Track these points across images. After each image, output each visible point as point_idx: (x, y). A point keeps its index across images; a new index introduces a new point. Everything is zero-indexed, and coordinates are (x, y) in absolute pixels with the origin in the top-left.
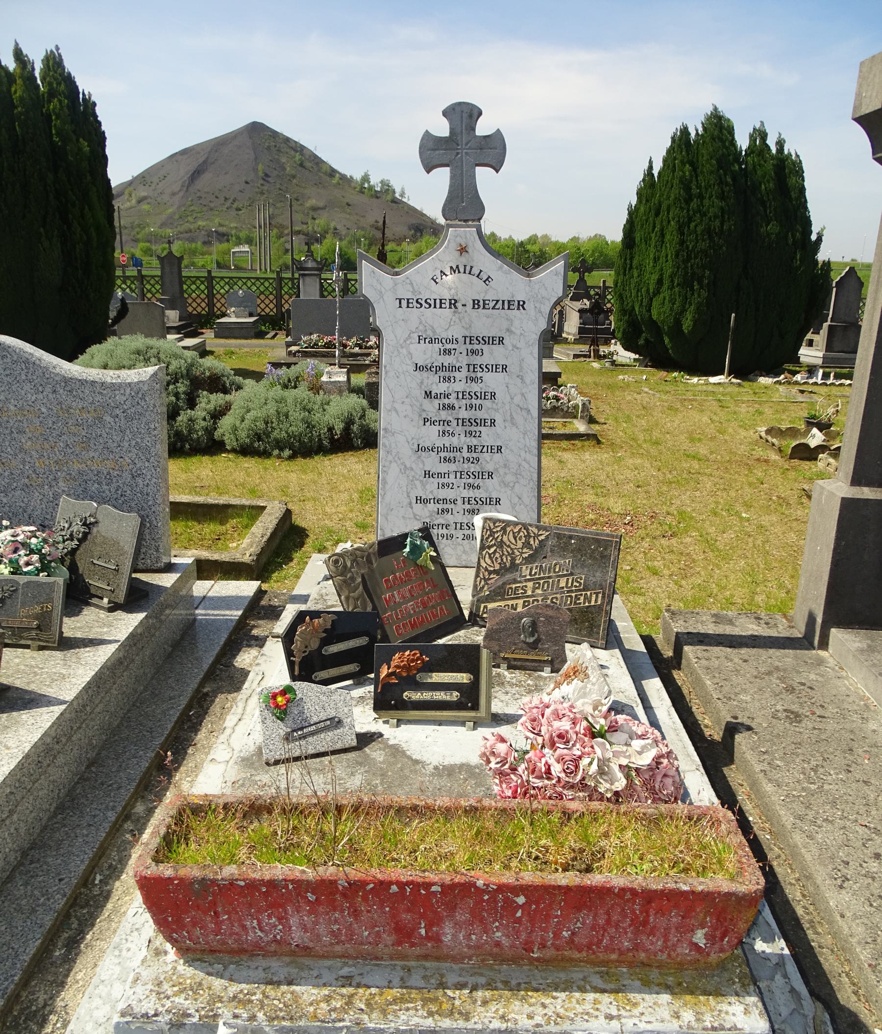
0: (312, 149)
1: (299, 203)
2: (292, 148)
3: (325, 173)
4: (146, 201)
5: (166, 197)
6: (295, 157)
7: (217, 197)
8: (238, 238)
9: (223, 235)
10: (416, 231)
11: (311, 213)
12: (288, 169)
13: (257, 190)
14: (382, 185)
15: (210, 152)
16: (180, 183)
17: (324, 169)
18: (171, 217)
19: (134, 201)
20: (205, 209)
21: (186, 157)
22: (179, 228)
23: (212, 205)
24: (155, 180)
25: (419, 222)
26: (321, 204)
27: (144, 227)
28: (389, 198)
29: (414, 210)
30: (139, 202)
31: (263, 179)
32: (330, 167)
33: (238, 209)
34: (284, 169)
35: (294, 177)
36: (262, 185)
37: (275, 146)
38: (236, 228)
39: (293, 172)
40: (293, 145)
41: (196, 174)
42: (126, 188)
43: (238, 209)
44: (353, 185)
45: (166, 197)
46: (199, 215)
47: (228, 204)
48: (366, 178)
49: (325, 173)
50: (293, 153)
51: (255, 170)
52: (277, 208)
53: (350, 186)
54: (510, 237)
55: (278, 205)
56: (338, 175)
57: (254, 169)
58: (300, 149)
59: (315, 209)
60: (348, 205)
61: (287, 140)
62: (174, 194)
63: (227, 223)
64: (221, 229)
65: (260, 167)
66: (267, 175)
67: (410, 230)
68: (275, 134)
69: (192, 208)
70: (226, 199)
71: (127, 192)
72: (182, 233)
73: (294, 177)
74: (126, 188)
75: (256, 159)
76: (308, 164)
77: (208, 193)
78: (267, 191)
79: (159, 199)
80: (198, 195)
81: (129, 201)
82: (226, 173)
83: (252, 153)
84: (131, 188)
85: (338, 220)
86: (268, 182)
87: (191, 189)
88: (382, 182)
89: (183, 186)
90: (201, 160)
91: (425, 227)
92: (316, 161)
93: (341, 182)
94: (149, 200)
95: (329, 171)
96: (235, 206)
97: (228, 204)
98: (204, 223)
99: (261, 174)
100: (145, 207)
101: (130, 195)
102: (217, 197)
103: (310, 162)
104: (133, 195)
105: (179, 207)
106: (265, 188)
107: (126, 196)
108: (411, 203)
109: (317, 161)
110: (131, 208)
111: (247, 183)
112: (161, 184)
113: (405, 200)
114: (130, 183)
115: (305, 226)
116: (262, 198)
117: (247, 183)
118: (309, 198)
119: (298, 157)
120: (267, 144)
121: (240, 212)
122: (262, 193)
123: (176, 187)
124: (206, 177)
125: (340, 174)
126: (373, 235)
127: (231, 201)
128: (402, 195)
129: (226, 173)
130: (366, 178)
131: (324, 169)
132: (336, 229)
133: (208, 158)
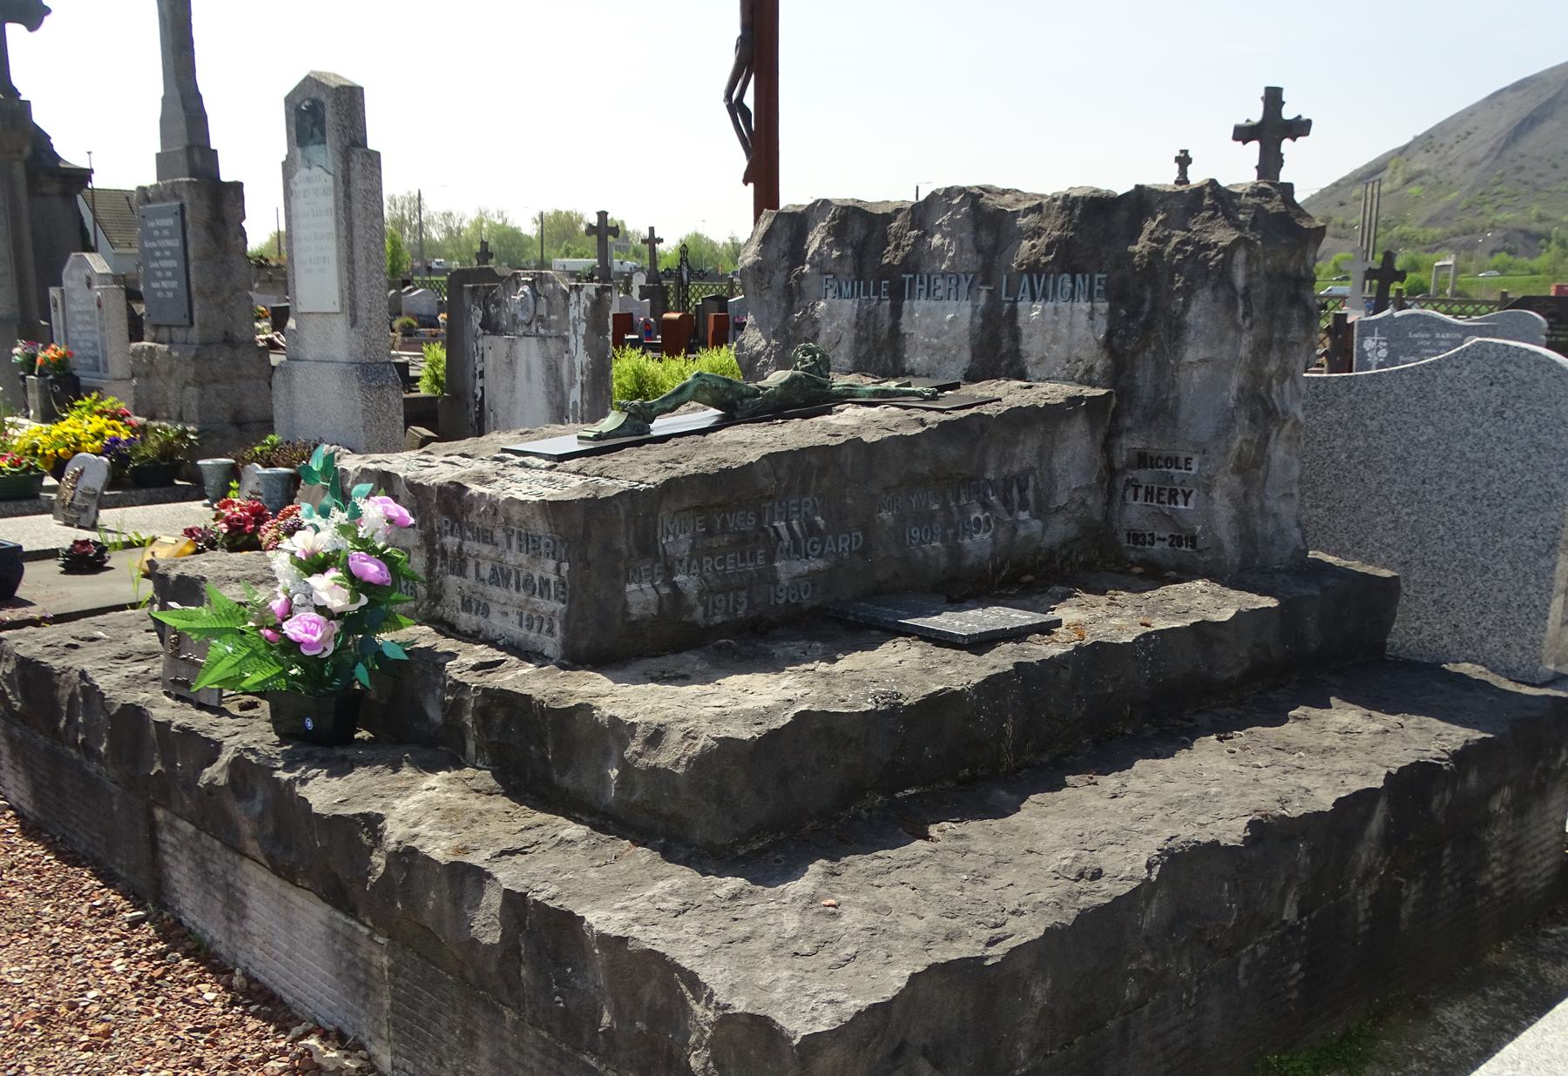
7: (1555, 166)
9: (1538, 237)
19: (1399, 180)
20: (1523, 190)
21: (1520, 93)
23: (1540, 181)
24: (1450, 140)
30: (1408, 181)
41: (1530, 123)
46: (1506, 201)
62: (1472, 165)
63: (1555, 214)
64: (1536, 227)
69: (1498, 188)
71: (1392, 164)
72: (1456, 235)
77: (1539, 159)
79: (1442, 176)
89: (1492, 149)
100: (1414, 190)
102: (1555, 166)
105: (1473, 189)
112: (1456, 148)
123: (1479, 153)
124: (1546, 129)
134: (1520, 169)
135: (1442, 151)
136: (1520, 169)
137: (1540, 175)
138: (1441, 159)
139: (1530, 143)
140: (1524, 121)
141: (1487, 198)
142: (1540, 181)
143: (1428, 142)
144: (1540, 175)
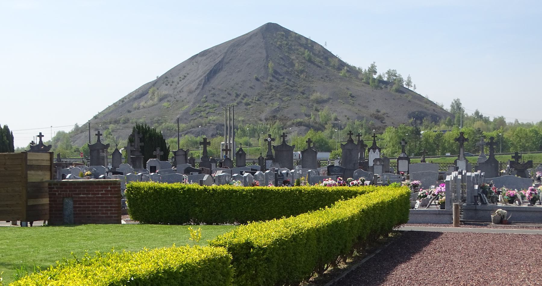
0: (323, 45)
1: (305, 96)
2: (301, 45)
3: (333, 67)
4: (166, 100)
5: (184, 95)
6: (304, 54)
7: (229, 94)
8: (243, 131)
10: (417, 119)
11: (315, 105)
12: (297, 65)
13: (266, 86)
14: (389, 75)
15: (226, 53)
16: (198, 81)
17: (332, 64)
18: (186, 113)
19: (156, 99)
20: (217, 105)
21: (205, 58)
22: (192, 123)
23: (224, 101)
24: (176, 79)
25: (420, 110)
26: (325, 97)
27: (162, 123)
28: (394, 87)
29: (420, 98)
30: (161, 100)
31: (273, 76)
32: (340, 61)
33: (247, 104)
34: (293, 65)
35: (302, 72)
36: (271, 81)
37: (287, 44)
38: (243, 121)
39: (301, 68)
40: (304, 42)
42: (150, 88)
43: (247, 104)
44: (360, 76)
45: (184, 95)
46: (211, 110)
47: (239, 99)
48: (373, 70)
49: (333, 67)
50: (302, 49)
51: (266, 67)
52: (283, 101)
53: (357, 78)
54: (517, 121)
55: (285, 99)
56: (345, 68)
57: (265, 66)
58: (309, 45)
59: (320, 102)
60: (353, 97)
61: (300, 37)
65: (271, 65)
66: (276, 72)
67: (410, 118)
68: (287, 33)
69: (206, 104)
70: (237, 96)
71: (151, 91)
72: (194, 127)
73: (302, 72)
74: (150, 88)
75: (267, 57)
76: (317, 60)
78: (276, 86)
80: (213, 92)
81: (152, 99)
82: (239, 71)
83: (264, 52)
84: (155, 88)
85: (340, 112)
86: (277, 79)
87: (207, 88)
88: (388, 72)
89: (199, 85)
90: (217, 61)
91: (426, 115)
92: (325, 55)
93: (347, 75)
94: (169, 98)
95: (337, 64)
96: (244, 101)
97: (239, 99)
98: (215, 118)
99: (270, 71)
100: (165, 104)
101: (153, 94)
102: (229, 94)
103: (319, 57)
104: (156, 94)
105: (194, 104)
106: (274, 84)
107: (149, 96)
108: (418, 91)
109: (326, 55)
110: (153, 105)
111: (257, 79)
113: (411, 88)
114: (154, 84)
115: (306, 118)
116: (270, 93)
117: (257, 79)
118: (314, 91)
119: (307, 53)
120: (279, 43)
121: (249, 107)
122: (271, 89)
123: (193, 86)
124: (221, 75)
125: (348, 66)
126: (373, 124)
127: (241, 96)
128: (408, 84)
129: (239, 71)
130: (373, 70)
131: (332, 64)
132: (336, 119)
133: (223, 58)
134: (214, 95)
135: (174, 84)
136: (214, 95)
137: (223, 98)
138: (174, 89)
139: (216, 82)
140: (211, 71)
141: (203, 109)
142: (224, 101)
143: (165, 79)
144: (223, 98)
